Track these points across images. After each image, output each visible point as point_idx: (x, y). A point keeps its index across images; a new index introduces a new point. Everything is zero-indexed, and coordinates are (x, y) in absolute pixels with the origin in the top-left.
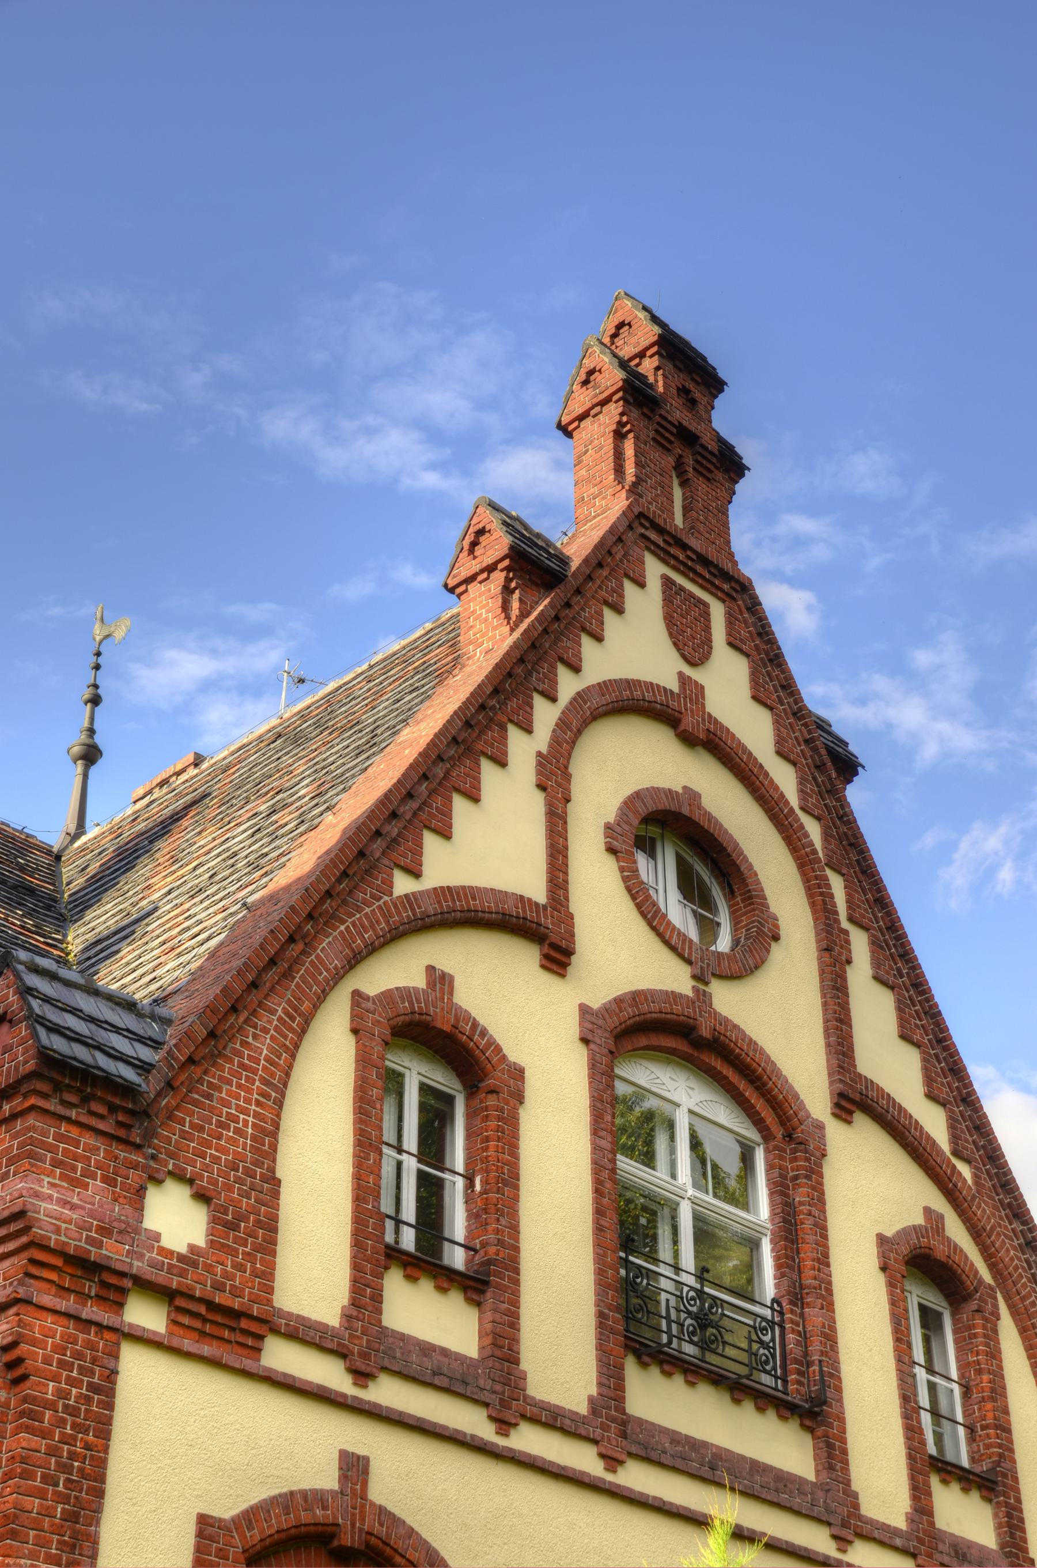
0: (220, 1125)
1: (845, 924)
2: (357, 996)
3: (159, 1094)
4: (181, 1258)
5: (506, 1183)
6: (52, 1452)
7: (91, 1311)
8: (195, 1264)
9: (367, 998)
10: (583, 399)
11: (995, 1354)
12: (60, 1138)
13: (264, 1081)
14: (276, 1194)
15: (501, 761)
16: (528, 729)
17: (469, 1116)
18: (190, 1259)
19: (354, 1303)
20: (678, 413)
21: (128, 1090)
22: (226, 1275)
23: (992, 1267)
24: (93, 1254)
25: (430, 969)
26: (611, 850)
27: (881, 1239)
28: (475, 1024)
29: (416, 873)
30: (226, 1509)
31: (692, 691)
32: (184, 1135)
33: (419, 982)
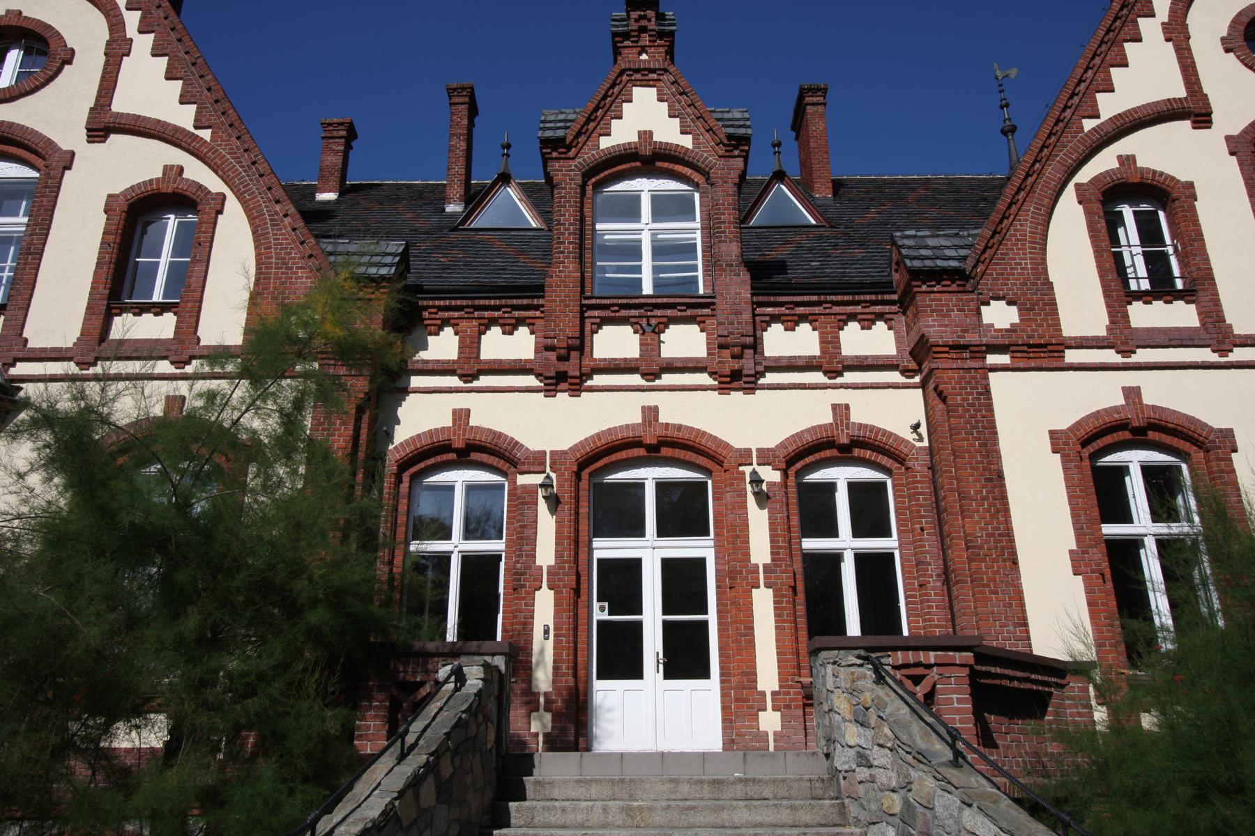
0: (1012, 269)
2: (1077, 185)
3: (975, 267)
4: (1007, 330)
5: (1194, 240)
6: (967, 422)
7: (970, 364)
8: (1015, 331)
9: (1083, 184)
12: (932, 300)
13: (1030, 242)
14: (1052, 289)
18: (1013, 328)
19: (1111, 322)
22: (1033, 330)
24: (962, 342)
25: (1119, 157)
28: (1154, 172)
30: (1064, 424)
32: (994, 279)
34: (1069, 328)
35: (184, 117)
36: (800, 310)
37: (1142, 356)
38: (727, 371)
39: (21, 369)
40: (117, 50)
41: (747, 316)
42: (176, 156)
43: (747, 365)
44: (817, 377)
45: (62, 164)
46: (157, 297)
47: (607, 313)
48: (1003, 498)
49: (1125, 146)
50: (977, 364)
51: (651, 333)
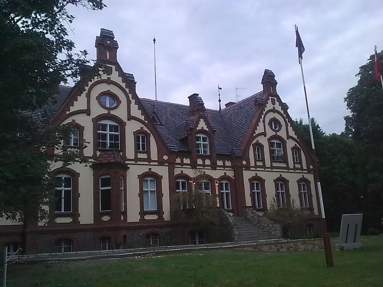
16: (262, 118)
23: (300, 146)
29: (255, 134)
33: (256, 141)
35: (142, 118)
39: (126, 162)
42: (142, 126)
46: (141, 150)
47: (199, 157)
49: (257, 139)
50: (242, 169)
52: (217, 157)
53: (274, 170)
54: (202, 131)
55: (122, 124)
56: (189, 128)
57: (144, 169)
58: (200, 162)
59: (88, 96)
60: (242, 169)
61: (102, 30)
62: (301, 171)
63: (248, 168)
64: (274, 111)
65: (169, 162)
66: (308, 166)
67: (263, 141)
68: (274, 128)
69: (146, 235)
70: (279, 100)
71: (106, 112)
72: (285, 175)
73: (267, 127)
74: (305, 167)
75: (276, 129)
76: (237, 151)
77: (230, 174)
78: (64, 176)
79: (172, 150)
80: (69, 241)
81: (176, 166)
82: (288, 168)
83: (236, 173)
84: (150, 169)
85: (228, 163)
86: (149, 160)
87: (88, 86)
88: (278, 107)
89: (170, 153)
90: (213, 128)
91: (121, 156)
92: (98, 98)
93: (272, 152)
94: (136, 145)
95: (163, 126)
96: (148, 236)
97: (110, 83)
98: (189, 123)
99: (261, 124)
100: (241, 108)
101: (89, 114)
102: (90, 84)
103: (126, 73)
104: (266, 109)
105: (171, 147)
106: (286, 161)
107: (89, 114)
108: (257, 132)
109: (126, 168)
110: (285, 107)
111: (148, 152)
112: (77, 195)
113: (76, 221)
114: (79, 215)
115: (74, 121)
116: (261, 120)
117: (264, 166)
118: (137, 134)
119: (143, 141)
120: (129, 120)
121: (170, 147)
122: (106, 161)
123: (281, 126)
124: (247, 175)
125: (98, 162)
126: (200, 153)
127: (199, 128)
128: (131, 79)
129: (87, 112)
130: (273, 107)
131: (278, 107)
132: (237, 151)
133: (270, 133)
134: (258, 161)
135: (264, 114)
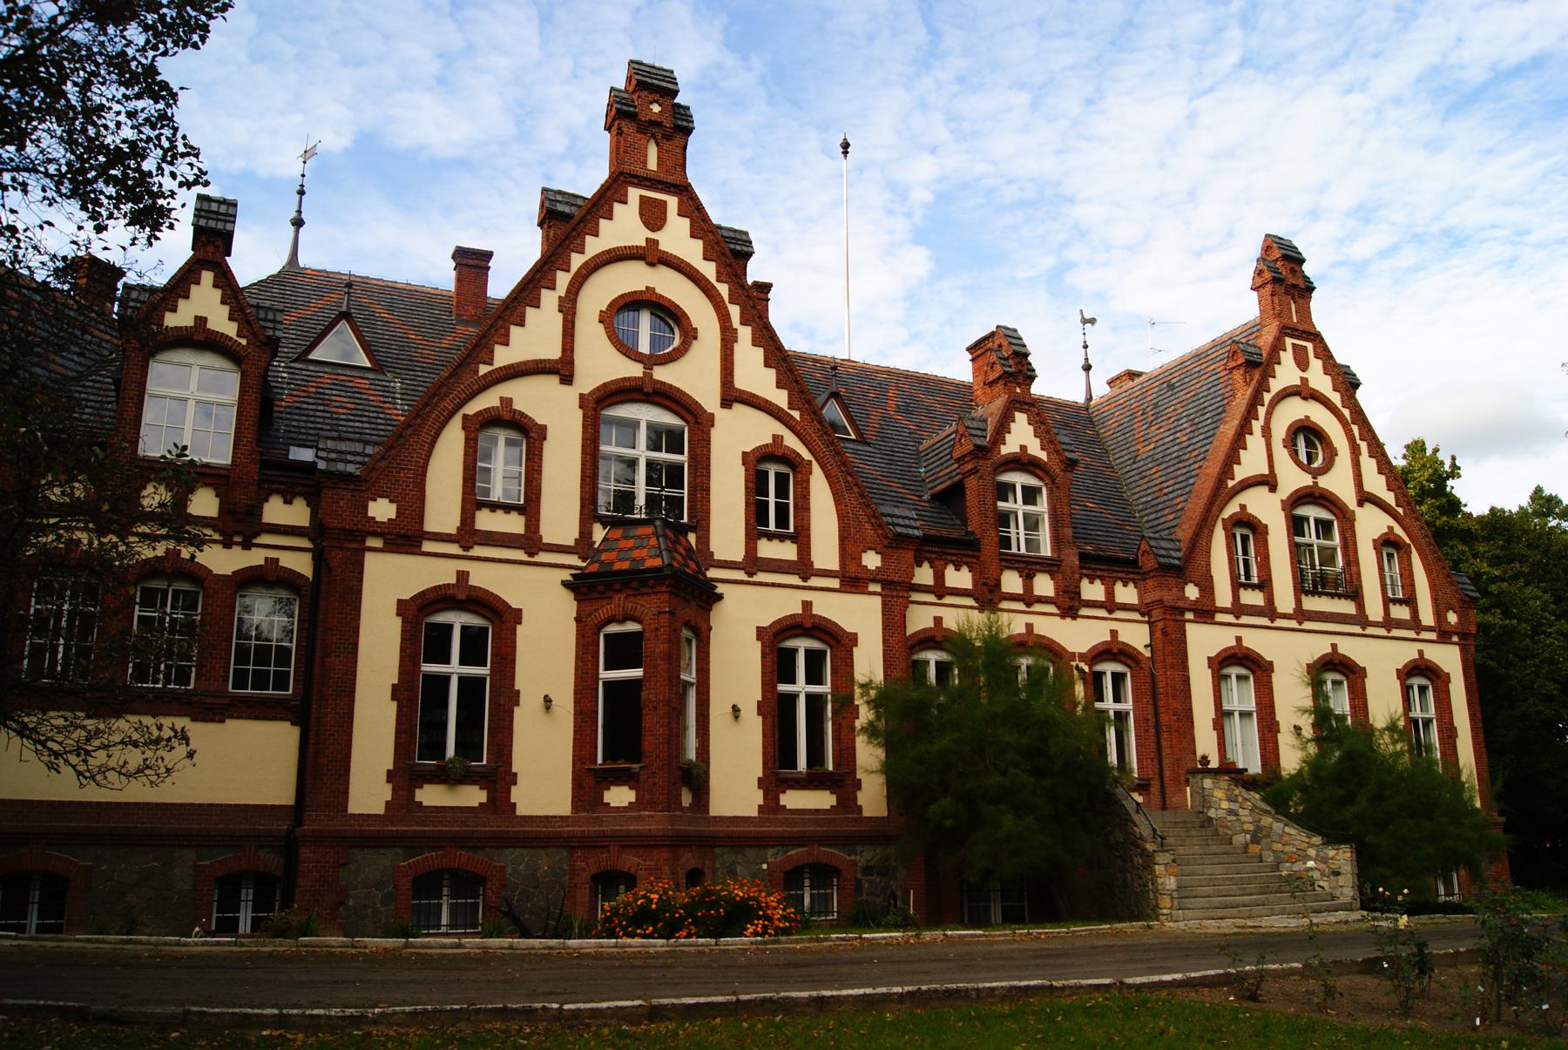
1: (1359, 442)
7: (1178, 618)
10: (1259, 281)
11: (1410, 564)
15: (1251, 434)
16: (1257, 419)
17: (1254, 540)
20: (1291, 280)
21: (1178, 566)
26: (1285, 447)
27: (1374, 540)
29: (1233, 479)
30: (1213, 655)
31: (1304, 381)
34: (1219, 604)
35: (780, 398)
36: (1098, 573)
37: (1245, 620)
38: (1067, 607)
39: (713, 573)
40: (728, 339)
41: (1077, 576)
43: (1076, 604)
44: (1103, 613)
45: (710, 423)
46: (772, 527)
48: (1189, 691)
49: (1243, 498)
51: (1028, 578)
52: (1081, 568)
53: (1307, 625)
54: (1022, 462)
55: (700, 421)
56: (971, 448)
57: (780, 603)
58: (1011, 582)
59: (568, 308)
60: (1181, 618)
61: (637, 66)
62: (1411, 634)
63: (1206, 613)
64: (1303, 392)
65: (886, 580)
66: (1439, 614)
67: (1266, 507)
68: (1303, 458)
69: (786, 873)
70: (1325, 354)
71: (635, 370)
72: (1352, 649)
73: (1282, 455)
74: (1427, 616)
75: (1315, 465)
76: (1163, 544)
77: (1136, 636)
78: (458, 620)
79: (899, 529)
80: (467, 883)
81: (916, 597)
82: (1361, 619)
83: (1158, 634)
84: (807, 605)
85: (1127, 594)
86: (804, 567)
87: (569, 271)
88: (1320, 381)
89: (892, 544)
90: (1066, 450)
91: (689, 549)
92: (606, 318)
93: (1297, 551)
94: (753, 508)
95: (868, 444)
96: (791, 879)
97: (655, 261)
98: (967, 427)
99: (1255, 441)
100: (1171, 387)
101: (567, 379)
102: (577, 261)
103: (719, 227)
104: (1276, 385)
105: (895, 520)
106: (1356, 595)
107: (567, 379)
108: (1241, 473)
109: (708, 597)
110: (1347, 382)
111: (802, 538)
112: (508, 698)
113: (500, 801)
114: (513, 779)
115: (507, 402)
116: (1257, 426)
117: (1269, 611)
118: (757, 462)
119: (782, 492)
120: (727, 403)
121: (889, 520)
122: (626, 565)
123: (1331, 454)
124: (1203, 642)
125: (595, 568)
126: (1014, 550)
127: (1010, 447)
128: (738, 248)
129: (563, 370)
130: (1302, 378)
131: (1320, 381)
132: (1163, 544)
133: (1292, 478)
134: (1246, 586)
135: (1267, 401)
